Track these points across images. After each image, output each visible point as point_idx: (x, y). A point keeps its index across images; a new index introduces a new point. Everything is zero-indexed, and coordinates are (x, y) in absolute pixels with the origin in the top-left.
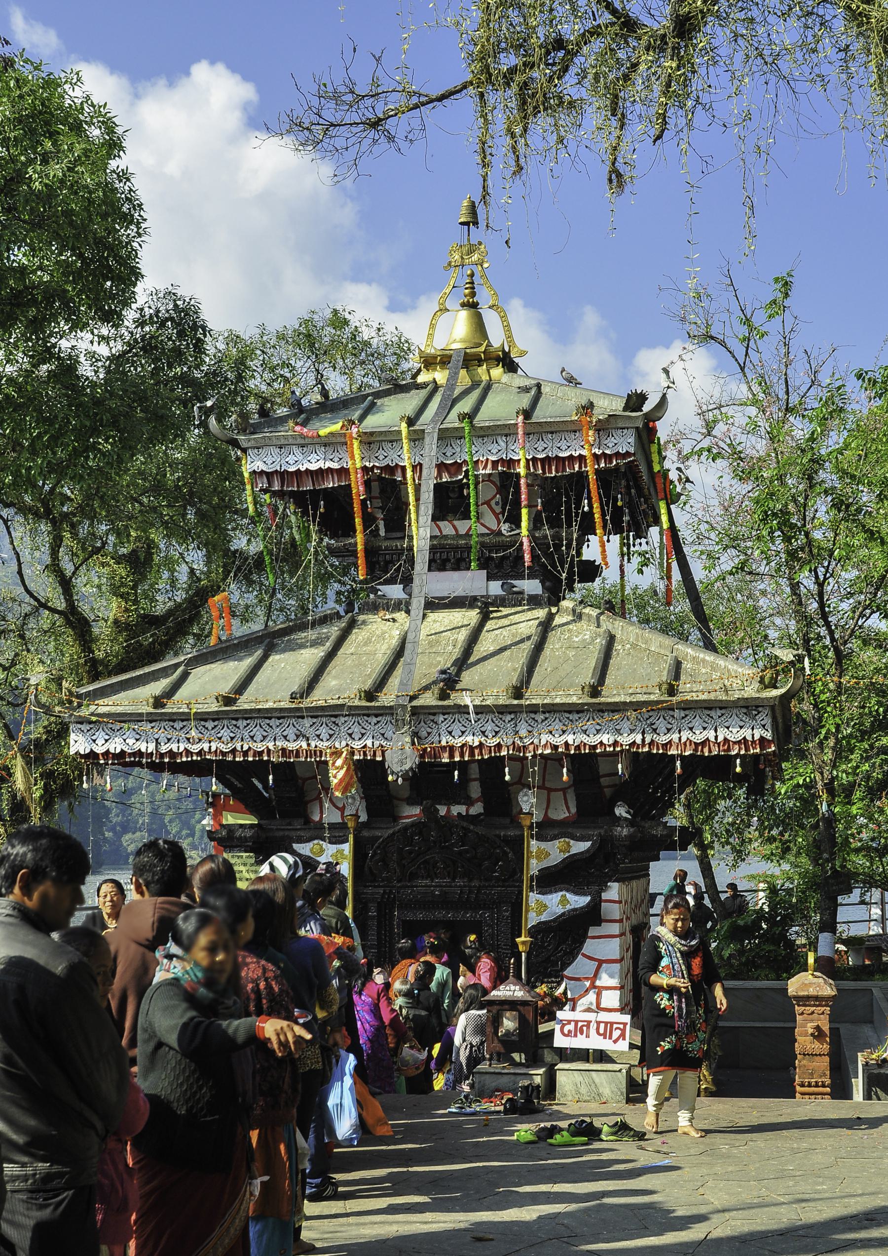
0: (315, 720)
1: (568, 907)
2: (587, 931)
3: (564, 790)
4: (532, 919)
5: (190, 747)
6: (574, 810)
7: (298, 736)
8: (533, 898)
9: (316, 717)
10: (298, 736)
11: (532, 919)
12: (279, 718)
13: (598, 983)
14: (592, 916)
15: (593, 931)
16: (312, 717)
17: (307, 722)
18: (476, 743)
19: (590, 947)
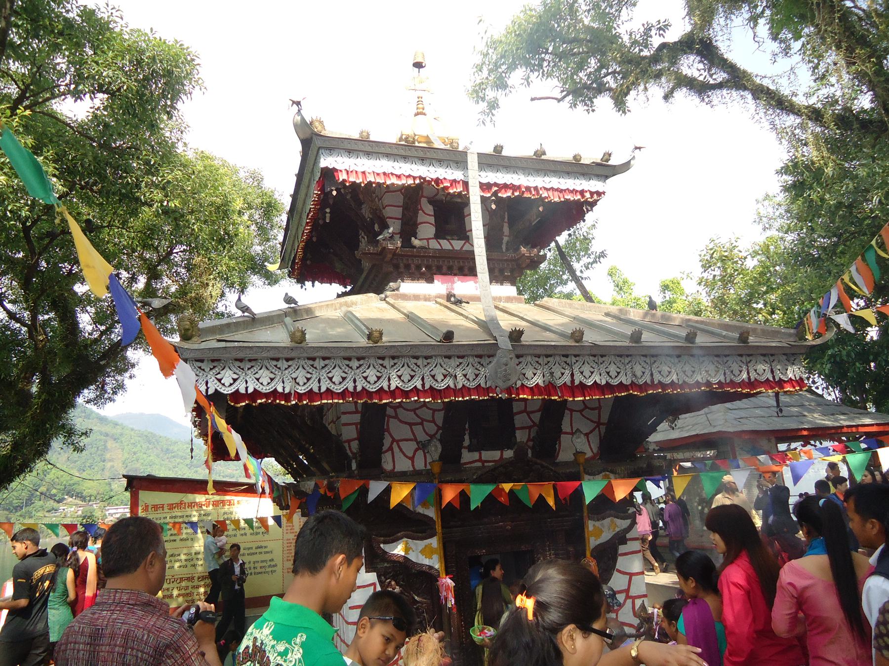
0: (461, 360)
1: (617, 530)
2: (616, 550)
3: (587, 435)
4: (593, 542)
5: (332, 387)
6: (595, 451)
7: (445, 376)
8: (591, 525)
9: (462, 357)
10: (445, 376)
11: (593, 542)
12: (426, 358)
13: (632, 593)
14: (621, 538)
15: (622, 549)
16: (459, 357)
17: (455, 362)
18: (604, 382)
19: (621, 563)
